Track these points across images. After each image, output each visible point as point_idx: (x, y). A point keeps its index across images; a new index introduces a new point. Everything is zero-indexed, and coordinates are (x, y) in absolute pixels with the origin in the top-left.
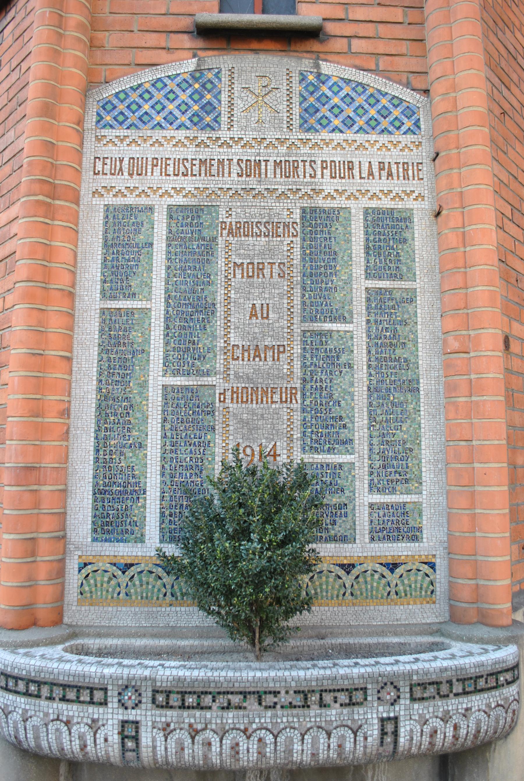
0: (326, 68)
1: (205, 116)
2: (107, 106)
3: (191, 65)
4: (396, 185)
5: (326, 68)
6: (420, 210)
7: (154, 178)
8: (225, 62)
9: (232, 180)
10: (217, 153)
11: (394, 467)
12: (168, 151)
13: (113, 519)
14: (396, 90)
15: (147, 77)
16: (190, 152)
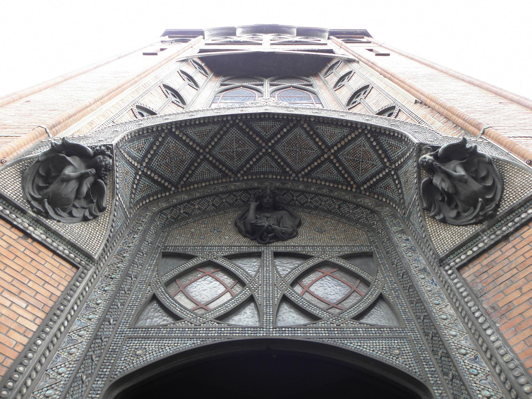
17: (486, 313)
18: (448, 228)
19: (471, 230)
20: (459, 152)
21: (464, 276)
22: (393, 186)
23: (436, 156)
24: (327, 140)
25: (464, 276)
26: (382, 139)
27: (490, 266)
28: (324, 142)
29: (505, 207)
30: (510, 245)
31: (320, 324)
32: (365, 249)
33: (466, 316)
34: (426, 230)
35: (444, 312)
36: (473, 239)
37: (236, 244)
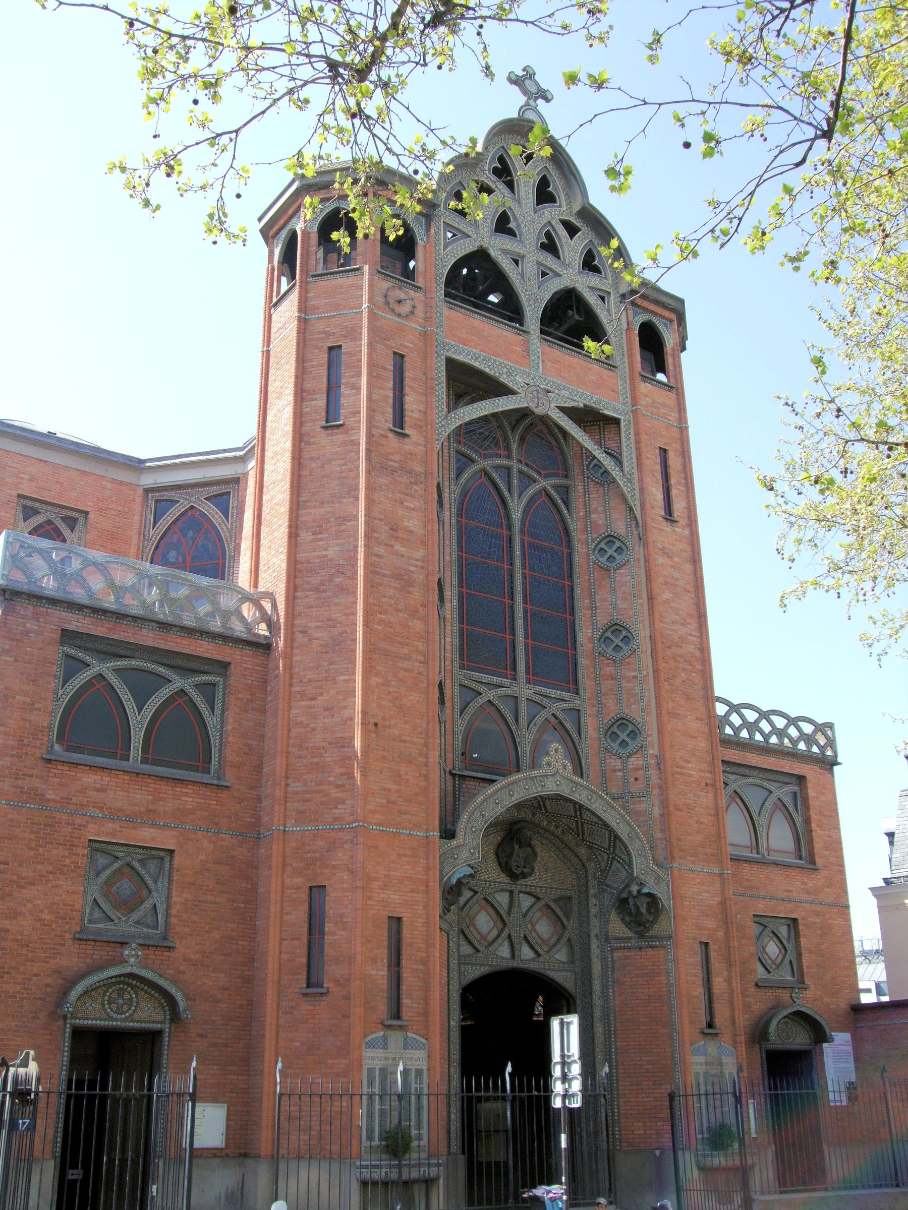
0: (409, 1034)
1: (385, 1046)
2: (367, 1043)
3: (382, 1033)
4: (420, 1063)
5: (409, 1034)
6: (425, 1068)
7: (376, 1061)
8: (389, 1033)
9: (390, 1062)
10: (388, 1055)
11: (419, 1126)
12: (380, 1055)
13: (370, 1137)
14: (422, 1039)
15: (374, 1036)
16: (383, 1055)
17: (613, 981)
18: (621, 923)
19: (629, 934)
20: (649, 895)
21: (615, 954)
22: (606, 859)
23: (639, 891)
24: (584, 817)
25: (615, 954)
26: (618, 843)
27: (627, 957)
28: (581, 815)
29: (650, 933)
30: (640, 953)
31: (540, 959)
32: (568, 893)
33: (604, 976)
34: (609, 915)
35: (597, 967)
36: (629, 938)
37: (498, 880)
